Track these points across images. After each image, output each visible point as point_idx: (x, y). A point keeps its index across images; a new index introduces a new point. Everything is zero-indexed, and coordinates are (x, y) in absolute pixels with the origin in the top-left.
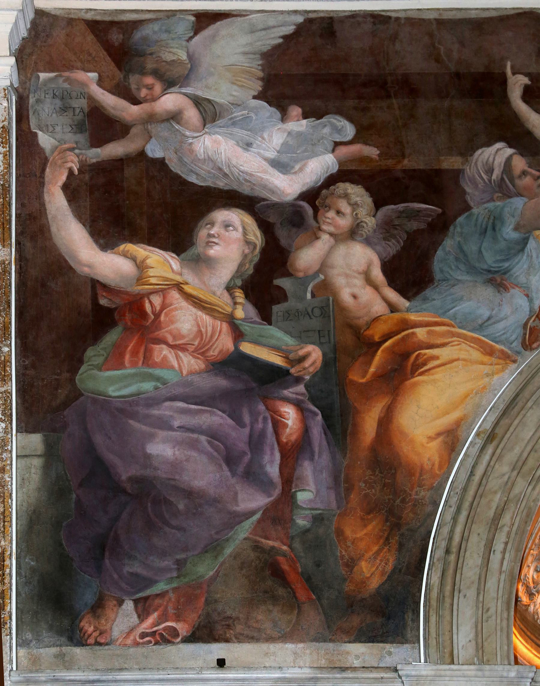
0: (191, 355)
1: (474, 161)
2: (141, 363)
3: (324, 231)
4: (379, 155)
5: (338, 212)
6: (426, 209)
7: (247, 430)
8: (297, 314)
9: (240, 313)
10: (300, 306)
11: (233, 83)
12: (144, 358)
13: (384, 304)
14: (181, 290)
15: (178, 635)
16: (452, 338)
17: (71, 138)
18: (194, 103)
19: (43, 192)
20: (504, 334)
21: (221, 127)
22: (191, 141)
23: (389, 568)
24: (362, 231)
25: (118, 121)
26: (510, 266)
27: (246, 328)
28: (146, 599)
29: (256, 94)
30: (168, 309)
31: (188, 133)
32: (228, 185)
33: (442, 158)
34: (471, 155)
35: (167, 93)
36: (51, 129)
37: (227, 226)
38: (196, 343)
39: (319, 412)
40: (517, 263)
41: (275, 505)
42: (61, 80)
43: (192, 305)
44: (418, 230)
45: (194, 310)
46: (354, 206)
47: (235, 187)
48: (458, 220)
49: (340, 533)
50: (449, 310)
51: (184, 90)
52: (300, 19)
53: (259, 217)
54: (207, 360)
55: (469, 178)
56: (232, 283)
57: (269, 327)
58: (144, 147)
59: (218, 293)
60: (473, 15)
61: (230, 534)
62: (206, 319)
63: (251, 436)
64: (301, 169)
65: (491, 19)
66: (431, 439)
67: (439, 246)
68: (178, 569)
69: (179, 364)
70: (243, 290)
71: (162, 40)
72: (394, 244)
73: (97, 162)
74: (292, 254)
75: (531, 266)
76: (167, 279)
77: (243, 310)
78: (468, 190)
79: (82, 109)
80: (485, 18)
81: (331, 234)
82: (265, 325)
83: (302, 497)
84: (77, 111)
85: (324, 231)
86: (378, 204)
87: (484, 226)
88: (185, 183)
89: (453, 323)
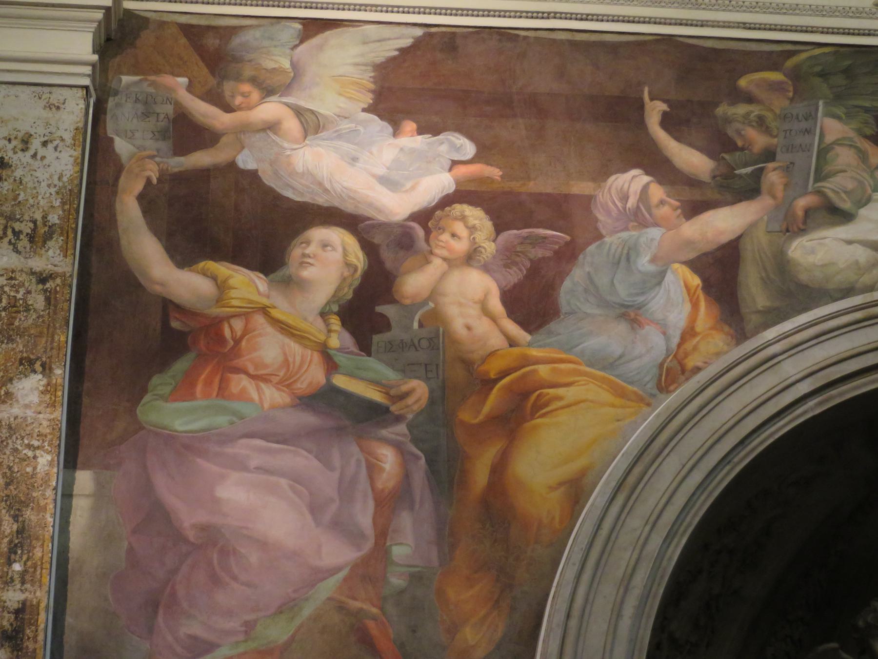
0: (275, 387)
1: (607, 188)
2: (215, 394)
3: (436, 255)
4: (501, 177)
5: (453, 235)
6: (553, 236)
7: (336, 475)
8: (401, 345)
9: (334, 342)
11: (340, 94)
12: (219, 388)
14: (266, 314)
17: (152, 145)
18: (294, 112)
19: (115, 201)
21: (324, 140)
22: (288, 153)
24: (479, 256)
25: (207, 129)
26: (645, 300)
27: (340, 359)
29: (366, 106)
30: (250, 335)
31: (286, 145)
32: (328, 201)
33: (572, 183)
34: (605, 180)
35: (266, 102)
36: (130, 134)
38: (282, 374)
40: (654, 298)
42: (145, 84)
43: (280, 331)
44: (544, 258)
45: (280, 337)
46: (472, 229)
47: (336, 203)
51: (284, 100)
52: (419, 32)
53: (363, 237)
54: (293, 393)
56: (328, 308)
57: (368, 358)
58: (235, 157)
59: (311, 319)
61: (310, 593)
62: (295, 348)
63: (341, 481)
64: (413, 188)
66: (552, 488)
67: (567, 276)
68: (246, 632)
69: (260, 398)
70: (340, 317)
71: (264, 47)
72: (515, 272)
73: (180, 172)
74: (398, 280)
77: (338, 338)
78: (601, 216)
79: (167, 115)
81: (445, 259)
82: (363, 356)
83: (399, 552)
84: (162, 116)
85: (436, 255)
86: (499, 228)
87: (617, 256)
88: (278, 198)
89: (580, 360)
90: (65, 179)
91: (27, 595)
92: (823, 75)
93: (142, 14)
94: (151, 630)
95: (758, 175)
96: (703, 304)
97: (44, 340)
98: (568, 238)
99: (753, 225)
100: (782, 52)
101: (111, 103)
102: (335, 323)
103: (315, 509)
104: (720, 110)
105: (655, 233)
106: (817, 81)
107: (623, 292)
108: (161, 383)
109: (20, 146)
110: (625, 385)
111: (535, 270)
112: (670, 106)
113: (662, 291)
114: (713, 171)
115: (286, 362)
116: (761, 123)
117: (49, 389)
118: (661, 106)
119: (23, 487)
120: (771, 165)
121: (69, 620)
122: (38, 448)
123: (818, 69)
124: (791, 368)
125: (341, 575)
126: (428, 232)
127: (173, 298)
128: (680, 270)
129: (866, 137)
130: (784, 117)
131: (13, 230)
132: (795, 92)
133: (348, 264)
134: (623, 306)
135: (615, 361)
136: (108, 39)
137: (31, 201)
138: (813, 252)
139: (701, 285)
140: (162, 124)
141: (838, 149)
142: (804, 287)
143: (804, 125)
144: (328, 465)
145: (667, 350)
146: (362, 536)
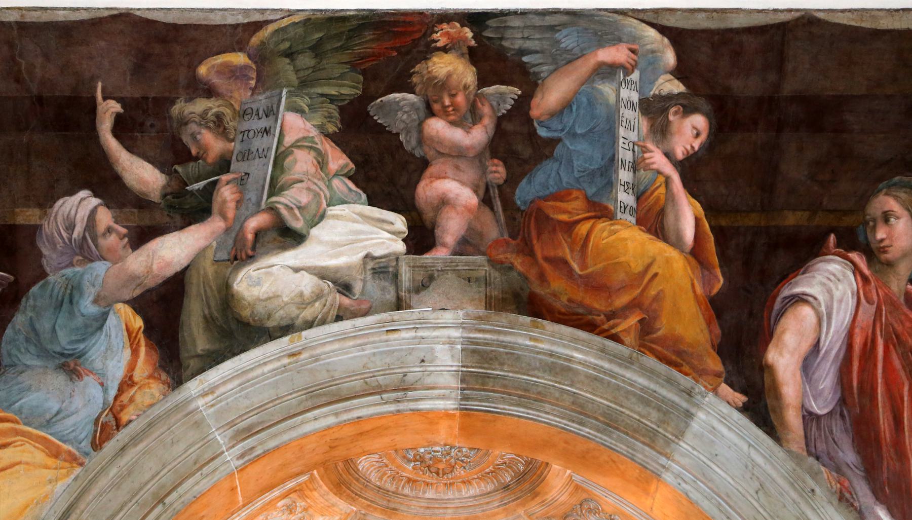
1: (53, 215)
16: (15, 436)
20: (73, 431)
33: (17, 210)
34: (51, 206)
40: (94, 344)
48: (31, 290)
50: (15, 403)
55: (46, 236)
60: (61, 17)
65: (82, 22)
75: (109, 348)
78: (45, 251)
80: (74, 22)
87: (60, 298)
92: (290, 54)
96: (143, 350)
99: (201, 254)
104: (176, 110)
105: (100, 268)
106: (284, 64)
107: (64, 339)
110: (60, 443)
113: (103, 337)
114: (164, 187)
116: (218, 124)
120: (224, 178)
128: (122, 311)
129: (328, 135)
135: (52, 418)
138: (258, 283)
139: (143, 329)
141: (296, 151)
142: (244, 325)
143: (263, 123)
145: (104, 403)
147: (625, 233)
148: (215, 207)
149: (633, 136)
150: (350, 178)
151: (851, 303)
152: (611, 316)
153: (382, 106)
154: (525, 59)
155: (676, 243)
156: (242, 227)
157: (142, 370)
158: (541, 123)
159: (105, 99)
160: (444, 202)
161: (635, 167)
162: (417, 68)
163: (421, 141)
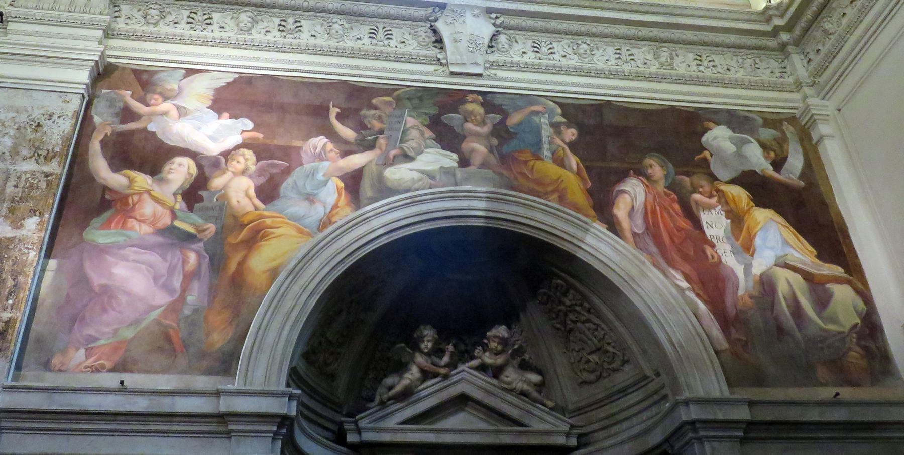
6: (282, 164)
7: (167, 264)
9: (178, 206)
10: (210, 205)
13: (252, 206)
15: (104, 368)
17: (110, 119)
23: (229, 337)
27: (179, 214)
28: (92, 348)
37: (180, 165)
38: (152, 219)
39: (208, 256)
41: (174, 302)
45: (153, 203)
46: (246, 159)
47: (189, 147)
49: (206, 317)
51: (173, 102)
52: (236, 76)
62: (159, 208)
63: (170, 266)
64: (223, 141)
66: (264, 272)
76: (144, 188)
78: (303, 156)
81: (233, 172)
83: (190, 299)
86: (259, 159)
88: (163, 143)
90: (65, 133)
91: (12, 314)
93: (117, 64)
94: (71, 330)
95: (375, 140)
97: (42, 202)
98: (288, 164)
99: (370, 161)
100: (393, 89)
101: (95, 101)
102: (179, 198)
103: (156, 279)
105: (326, 164)
107: (309, 189)
108: (96, 222)
109: (48, 118)
111: (271, 178)
112: (341, 110)
114: (356, 137)
115: (154, 215)
116: (380, 119)
117: (41, 223)
118: (338, 110)
119: (20, 267)
120: (381, 136)
121: (33, 326)
122: (30, 249)
123: (407, 96)
124: (376, 223)
125: (162, 308)
126: (227, 160)
127: (109, 187)
130: (389, 116)
131: (38, 153)
132: (397, 104)
133: (189, 173)
134: (308, 194)
136: (99, 74)
137: (48, 142)
140: (117, 110)
141: (412, 130)
143: (397, 120)
144: (166, 261)
146: (175, 291)
147: (549, 165)
148: (377, 146)
149: (548, 134)
150: (434, 140)
151: (643, 194)
152: (546, 193)
153: (446, 117)
154: (503, 107)
155: (570, 170)
156: (388, 153)
157: (343, 201)
158: (511, 128)
159: (333, 107)
160: (473, 151)
161: (550, 143)
162: (460, 107)
163: (462, 130)
